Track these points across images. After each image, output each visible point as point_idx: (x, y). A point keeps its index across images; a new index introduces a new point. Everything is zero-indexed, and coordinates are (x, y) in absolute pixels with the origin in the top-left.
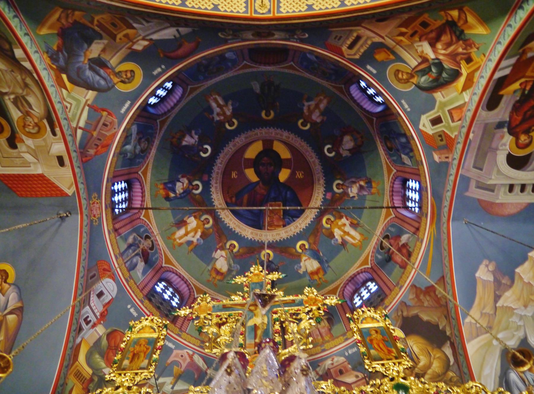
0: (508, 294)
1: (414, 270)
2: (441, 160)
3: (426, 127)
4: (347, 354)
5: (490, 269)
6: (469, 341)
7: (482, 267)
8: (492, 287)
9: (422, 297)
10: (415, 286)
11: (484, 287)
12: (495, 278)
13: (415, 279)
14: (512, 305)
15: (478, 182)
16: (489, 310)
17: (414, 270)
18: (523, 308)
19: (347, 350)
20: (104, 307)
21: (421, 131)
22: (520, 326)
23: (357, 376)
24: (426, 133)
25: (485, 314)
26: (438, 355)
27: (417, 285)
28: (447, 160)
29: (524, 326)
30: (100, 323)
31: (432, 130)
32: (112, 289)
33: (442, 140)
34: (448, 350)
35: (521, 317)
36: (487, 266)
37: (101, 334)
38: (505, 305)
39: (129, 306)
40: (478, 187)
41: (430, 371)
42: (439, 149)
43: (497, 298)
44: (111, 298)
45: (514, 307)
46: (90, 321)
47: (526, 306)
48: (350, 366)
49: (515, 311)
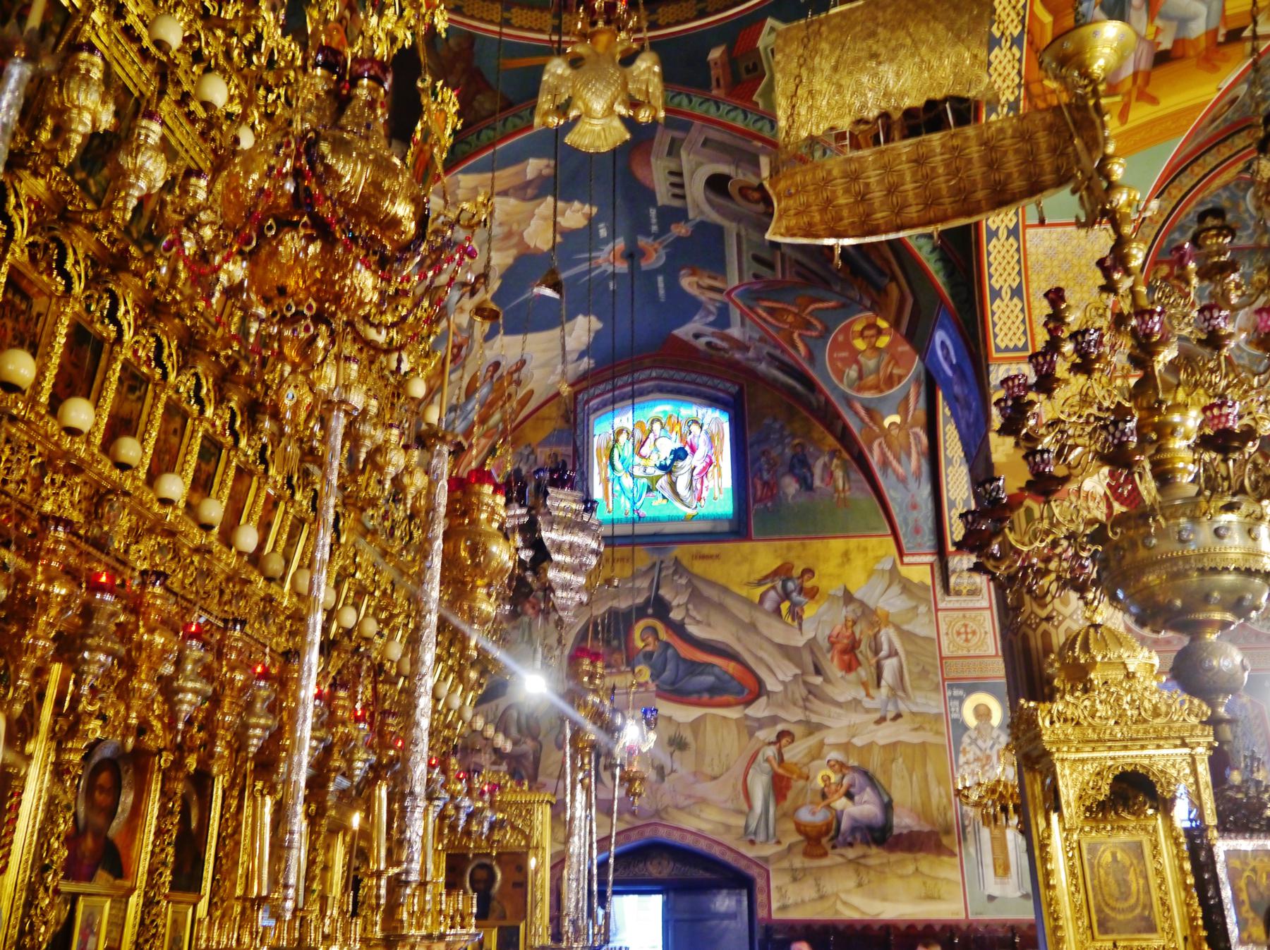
1: (497, 29)
2: (712, 64)
3: (769, 33)
7: (543, 162)
8: (517, 181)
9: (459, 66)
10: (472, 44)
11: (517, 174)
12: (531, 182)
13: (485, 38)
15: (683, 140)
17: (497, 29)
21: (764, 20)
24: (760, 33)
27: (476, 47)
28: (714, 83)
31: (766, 48)
33: (748, 71)
36: (548, 166)
40: (673, 141)
42: (731, 60)
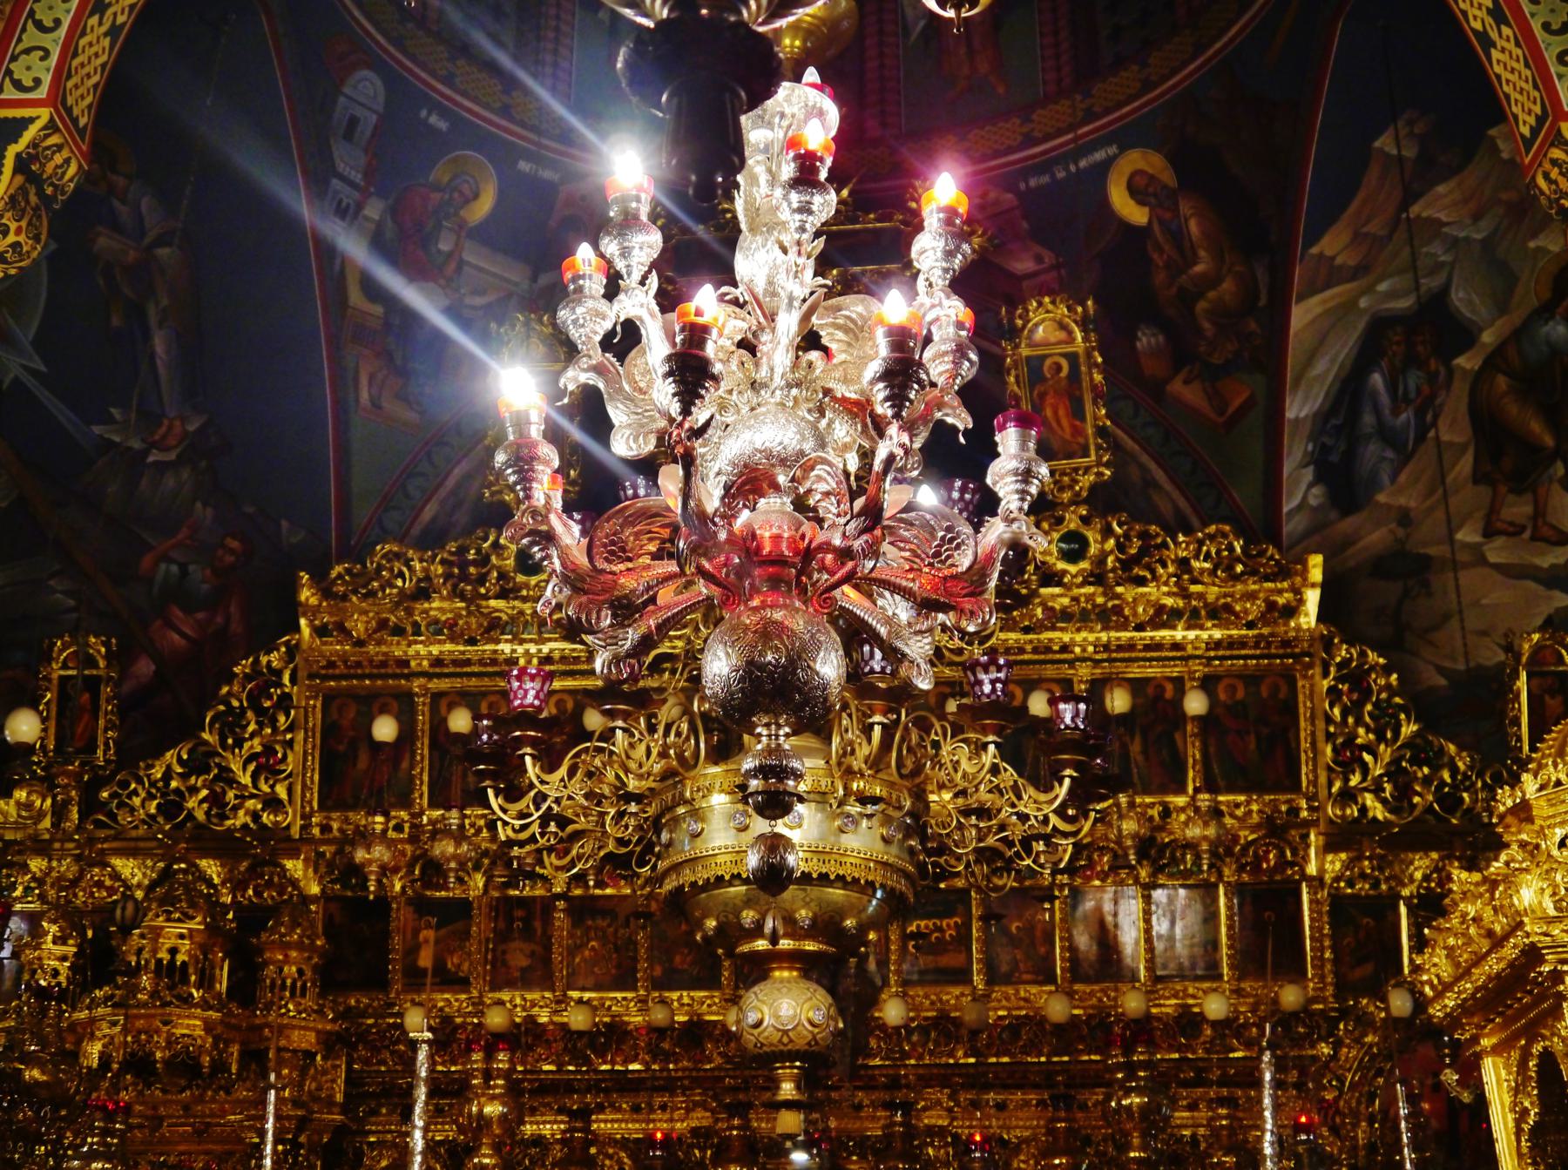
0: (1441, 189)
4: (1022, 186)
5: (1416, 131)
6: (1301, 298)
14: (1443, 217)
16: (1375, 227)
18: (1468, 221)
19: (1025, 173)
20: (366, 151)
22: (1443, 264)
23: (1039, 259)
25: (1366, 235)
26: (1238, 268)
29: (1452, 264)
30: (371, 194)
32: (371, 93)
34: (1262, 276)
35: (1455, 243)
36: (1411, 123)
37: (377, 217)
38: (1424, 214)
39: (424, 113)
41: (1212, 294)
43: (1409, 198)
44: (375, 117)
45: (1445, 219)
46: (348, 205)
47: (1476, 217)
48: (1025, 225)
49: (1445, 230)
